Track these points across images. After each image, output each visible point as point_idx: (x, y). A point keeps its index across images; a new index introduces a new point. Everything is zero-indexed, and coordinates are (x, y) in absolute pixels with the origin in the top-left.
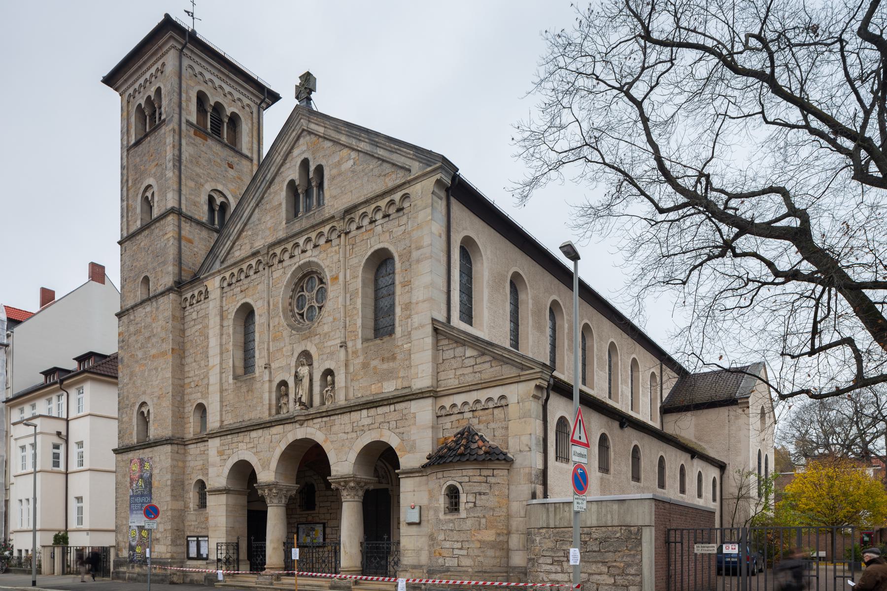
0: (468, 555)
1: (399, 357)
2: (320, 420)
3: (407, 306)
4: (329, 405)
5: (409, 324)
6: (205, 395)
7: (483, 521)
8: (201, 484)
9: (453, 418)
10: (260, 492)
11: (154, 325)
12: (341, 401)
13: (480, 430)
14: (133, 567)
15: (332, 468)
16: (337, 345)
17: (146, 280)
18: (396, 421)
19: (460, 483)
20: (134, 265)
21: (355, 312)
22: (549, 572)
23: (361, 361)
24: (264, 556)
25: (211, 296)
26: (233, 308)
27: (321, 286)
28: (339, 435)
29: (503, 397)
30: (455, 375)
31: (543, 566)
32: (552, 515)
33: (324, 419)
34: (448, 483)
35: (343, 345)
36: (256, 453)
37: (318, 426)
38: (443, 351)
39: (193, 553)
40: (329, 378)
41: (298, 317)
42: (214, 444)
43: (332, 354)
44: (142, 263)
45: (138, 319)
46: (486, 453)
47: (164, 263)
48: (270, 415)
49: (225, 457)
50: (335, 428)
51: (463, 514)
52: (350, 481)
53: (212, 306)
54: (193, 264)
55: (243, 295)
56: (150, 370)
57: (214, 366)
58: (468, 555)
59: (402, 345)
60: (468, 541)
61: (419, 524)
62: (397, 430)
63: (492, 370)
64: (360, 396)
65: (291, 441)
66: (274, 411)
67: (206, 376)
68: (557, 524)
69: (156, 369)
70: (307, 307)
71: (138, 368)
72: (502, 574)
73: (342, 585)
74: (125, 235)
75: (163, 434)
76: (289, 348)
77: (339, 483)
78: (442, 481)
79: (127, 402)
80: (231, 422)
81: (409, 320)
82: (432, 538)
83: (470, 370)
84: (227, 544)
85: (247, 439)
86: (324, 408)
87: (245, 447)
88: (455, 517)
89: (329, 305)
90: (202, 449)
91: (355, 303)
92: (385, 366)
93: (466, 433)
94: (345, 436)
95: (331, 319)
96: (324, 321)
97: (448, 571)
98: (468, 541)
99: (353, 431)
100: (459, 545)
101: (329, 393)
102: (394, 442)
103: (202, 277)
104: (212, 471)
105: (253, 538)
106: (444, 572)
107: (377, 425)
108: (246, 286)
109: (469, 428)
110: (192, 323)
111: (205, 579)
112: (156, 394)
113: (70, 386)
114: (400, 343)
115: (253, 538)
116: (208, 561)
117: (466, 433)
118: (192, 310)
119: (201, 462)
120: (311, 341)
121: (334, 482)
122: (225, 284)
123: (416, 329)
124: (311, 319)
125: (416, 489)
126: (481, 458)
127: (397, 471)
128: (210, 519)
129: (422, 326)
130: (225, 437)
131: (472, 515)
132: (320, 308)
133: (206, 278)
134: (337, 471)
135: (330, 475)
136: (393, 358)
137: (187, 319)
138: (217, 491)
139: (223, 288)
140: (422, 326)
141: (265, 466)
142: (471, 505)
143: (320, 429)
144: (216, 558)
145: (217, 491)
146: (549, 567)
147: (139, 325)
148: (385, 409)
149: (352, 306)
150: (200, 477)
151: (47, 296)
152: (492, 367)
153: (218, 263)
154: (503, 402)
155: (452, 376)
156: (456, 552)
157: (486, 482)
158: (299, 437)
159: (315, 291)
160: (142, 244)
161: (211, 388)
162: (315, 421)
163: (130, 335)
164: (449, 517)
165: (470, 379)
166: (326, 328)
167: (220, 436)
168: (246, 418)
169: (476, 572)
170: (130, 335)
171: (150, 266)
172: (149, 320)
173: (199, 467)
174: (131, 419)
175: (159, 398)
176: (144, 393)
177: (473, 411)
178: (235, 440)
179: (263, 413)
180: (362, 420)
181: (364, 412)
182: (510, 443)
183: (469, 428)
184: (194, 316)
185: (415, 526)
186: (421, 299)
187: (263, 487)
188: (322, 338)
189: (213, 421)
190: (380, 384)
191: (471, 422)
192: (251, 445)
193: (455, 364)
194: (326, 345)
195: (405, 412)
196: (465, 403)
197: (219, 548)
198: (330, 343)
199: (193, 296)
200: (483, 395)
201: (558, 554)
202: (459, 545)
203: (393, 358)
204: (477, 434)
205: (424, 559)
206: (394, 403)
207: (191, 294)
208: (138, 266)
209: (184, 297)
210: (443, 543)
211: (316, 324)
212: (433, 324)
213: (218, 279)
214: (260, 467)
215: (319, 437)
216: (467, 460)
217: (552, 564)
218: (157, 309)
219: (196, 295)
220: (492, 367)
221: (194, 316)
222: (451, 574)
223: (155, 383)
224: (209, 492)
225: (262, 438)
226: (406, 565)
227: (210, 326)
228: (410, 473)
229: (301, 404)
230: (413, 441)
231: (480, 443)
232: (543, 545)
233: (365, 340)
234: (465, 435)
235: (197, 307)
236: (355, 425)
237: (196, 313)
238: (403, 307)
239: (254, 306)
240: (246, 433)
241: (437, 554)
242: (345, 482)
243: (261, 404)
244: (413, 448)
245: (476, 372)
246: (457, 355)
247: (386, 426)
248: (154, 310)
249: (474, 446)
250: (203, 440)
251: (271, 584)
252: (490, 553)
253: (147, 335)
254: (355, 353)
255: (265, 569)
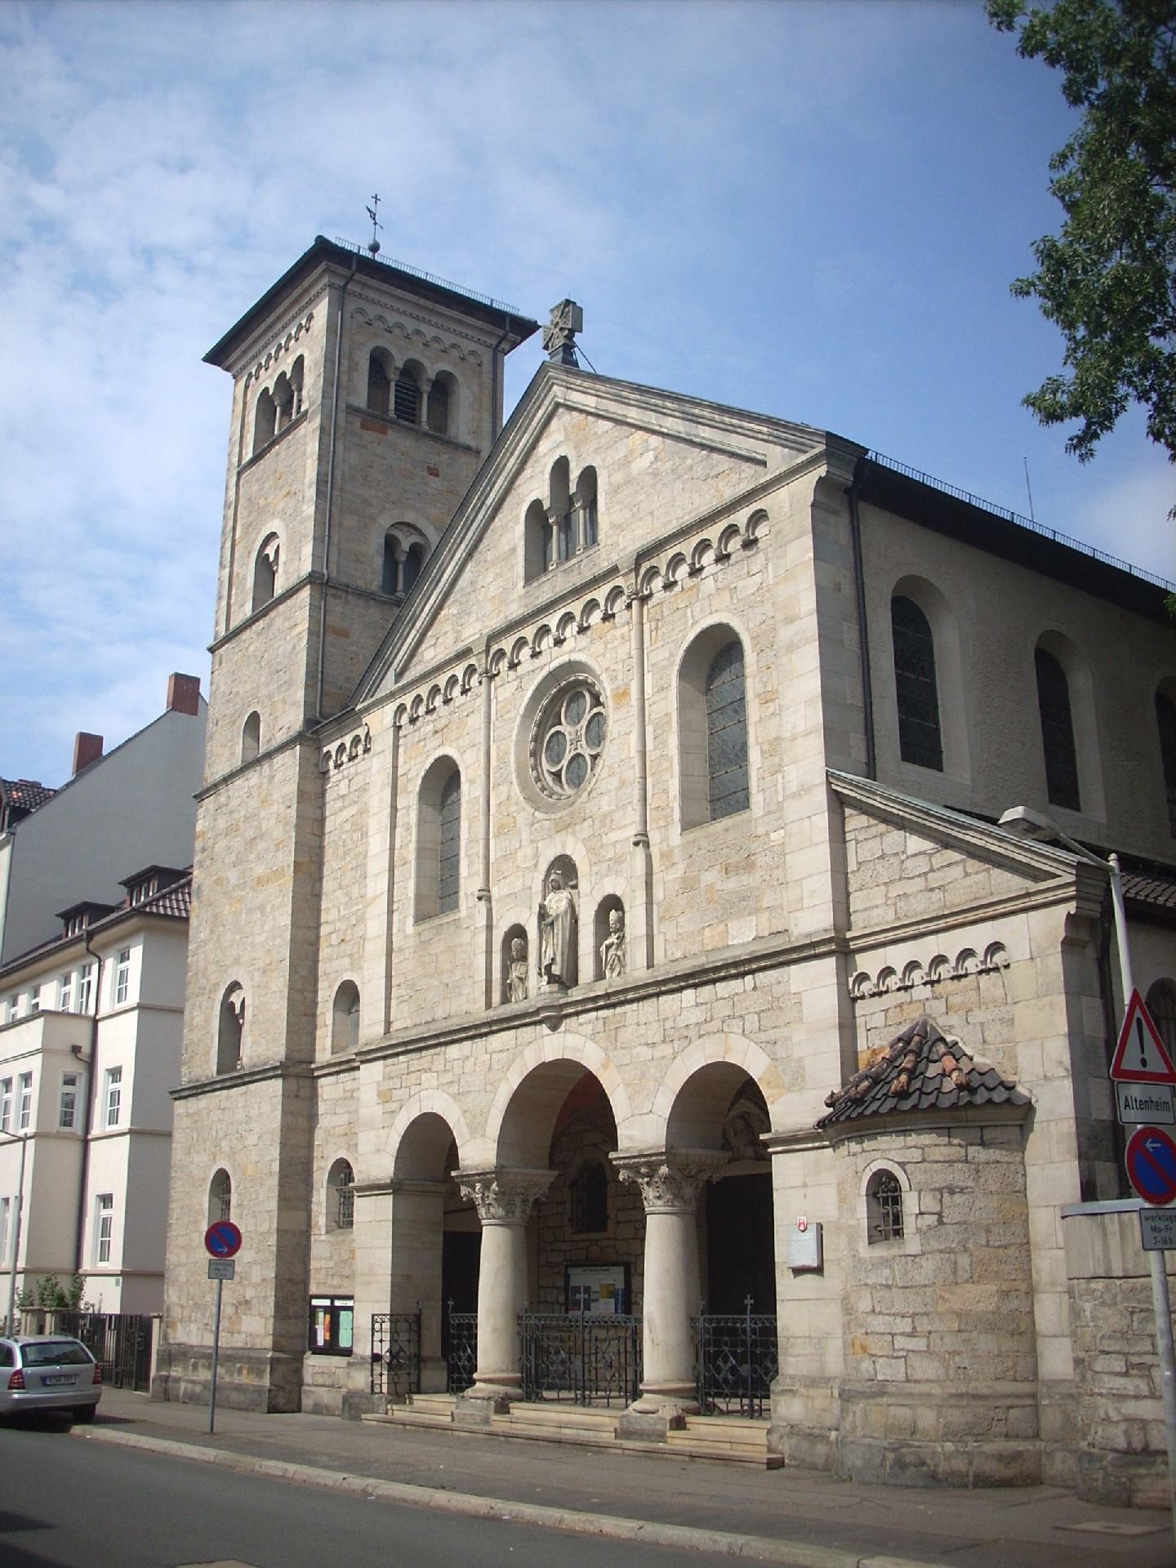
0: (928, 1352)
1: (760, 860)
2: (593, 1015)
3: (774, 747)
4: (613, 981)
5: (780, 787)
6: (356, 962)
7: (964, 1261)
8: (342, 1171)
9: (887, 1000)
10: (464, 1191)
11: (263, 814)
12: (637, 970)
13: (951, 1028)
14: (195, 1367)
15: (621, 1132)
16: (627, 839)
17: (254, 721)
18: (758, 1013)
19: (902, 1165)
20: (234, 690)
21: (665, 765)
22: (1120, 1397)
23: (680, 873)
24: (474, 1349)
25: (375, 747)
26: (415, 769)
27: (595, 710)
28: (634, 1051)
29: (995, 947)
30: (887, 898)
31: (1106, 1378)
32: (1114, 1243)
33: (602, 1013)
34: (875, 1167)
35: (643, 841)
36: (457, 1097)
37: (588, 1029)
38: (857, 842)
39: (322, 1337)
40: (613, 915)
41: (549, 779)
42: (371, 1073)
43: (618, 860)
44: (248, 687)
45: (234, 803)
46: (960, 1087)
47: (289, 683)
48: (488, 1005)
49: (393, 1106)
50: (626, 1035)
51: (912, 1243)
52: (661, 1163)
53: (376, 766)
54: (348, 679)
55: (438, 739)
56: (250, 911)
57: (375, 898)
58: (928, 1352)
59: (767, 834)
60: (927, 1314)
61: (818, 1270)
62: (763, 1036)
63: (969, 880)
64: (679, 954)
65: (531, 1066)
66: (496, 997)
67: (361, 920)
68: (1130, 1266)
69: (262, 908)
70: (568, 757)
71: (228, 907)
72: (1019, 1402)
73: (646, 1427)
74: (223, 633)
75: (270, 1054)
76: (529, 850)
77: (635, 1168)
78: (860, 1162)
79: (203, 982)
80: (409, 1023)
81: (780, 776)
82: (847, 1308)
83: (920, 883)
84: (394, 1318)
85: (439, 1065)
86: (601, 989)
87: (435, 1083)
88: (894, 1251)
89: (611, 751)
90: (349, 1086)
91: (665, 743)
92: (732, 884)
93: (916, 1039)
94: (646, 1053)
95: (614, 782)
96: (602, 787)
97: (882, 1394)
98: (927, 1314)
99: (664, 1042)
100: (905, 1325)
101: (612, 951)
102: (756, 1066)
103: (359, 707)
104: (366, 1140)
105: (451, 1303)
106: (874, 1396)
107: (716, 1025)
108: (444, 721)
109: (925, 1024)
110: (339, 804)
111: (344, 1404)
112: (260, 964)
113: (105, 946)
114: (761, 830)
115: (451, 1303)
116: (351, 1359)
117: (916, 1039)
118: (339, 777)
119: (345, 1118)
120: (574, 834)
121: (625, 1166)
122: (405, 719)
123: (794, 795)
124: (577, 781)
125: (808, 1181)
126: (945, 1102)
127: (763, 1137)
128: (358, 1254)
129: (805, 790)
130: (395, 1060)
131: (935, 1245)
132: (595, 757)
133: (367, 709)
134: (631, 1138)
135: (615, 1148)
136: (748, 864)
137: (329, 796)
138: (374, 1188)
139: (400, 727)
140: (805, 790)
141: (476, 1130)
142: (931, 1220)
143: (593, 1037)
144: (369, 1353)
145: (374, 1188)
146: (1119, 1382)
147: (235, 815)
148: (735, 985)
149: (658, 753)
150: (342, 1154)
151: (89, 749)
152: (967, 874)
153: (391, 675)
154: (999, 958)
155: (881, 901)
156: (900, 1342)
157: (966, 1161)
158: (549, 1057)
159: (584, 723)
160: (252, 648)
161: (369, 947)
162: (584, 1018)
163: (217, 835)
164: (881, 1251)
165: (922, 906)
166: (605, 804)
167: (385, 1058)
168: (440, 1013)
169: (952, 1396)
170: (217, 835)
171: (263, 692)
172: (254, 803)
173: (341, 1131)
174: (207, 1021)
175: (265, 972)
176: (237, 961)
177: (932, 983)
178: (415, 1065)
179: (470, 1005)
180: (685, 1013)
181: (689, 994)
182: (1020, 1059)
183: (925, 1024)
184: (343, 788)
185: (809, 1276)
186: (800, 728)
187: (469, 1181)
188: (597, 824)
189: (371, 1024)
190: (722, 927)
191: (928, 1011)
192: (448, 1077)
193: (884, 872)
194: (605, 839)
195: (778, 990)
196: (913, 966)
197: (377, 1326)
198: (613, 837)
199: (342, 748)
200: (950, 944)
201: (1139, 1348)
202: (905, 1325)
203: (748, 864)
204: (942, 1040)
205: (834, 1363)
206: (752, 972)
207: (338, 742)
208: (242, 691)
209: (325, 750)
210: (870, 1318)
211: (586, 793)
212: (829, 783)
213: (390, 708)
214: (465, 1130)
215: (591, 1058)
216: (915, 1107)
217: (1126, 1374)
218: (272, 777)
219: (348, 745)
220: (967, 874)
221: (343, 788)
222: (892, 1400)
223: (259, 939)
224: (359, 1189)
225: (472, 1060)
226: (792, 1377)
227: (371, 811)
228: (793, 1141)
229: (552, 979)
230: (800, 1060)
231: (948, 1062)
232: (1100, 1323)
233: (687, 825)
234: (912, 1046)
235: (349, 768)
236: (668, 1024)
237: (346, 781)
238: (766, 747)
239: (459, 762)
240: (438, 1050)
241: (858, 1348)
242: (649, 1164)
243: (469, 982)
244: (797, 1081)
245: (932, 890)
246: (888, 851)
247: (736, 1025)
248: (265, 781)
249: (933, 1070)
250: (349, 1067)
251: (486, 1421)
252: (986, 1343)
253: (250, 834)
254: (666, 855)
255: (472, 1382)
